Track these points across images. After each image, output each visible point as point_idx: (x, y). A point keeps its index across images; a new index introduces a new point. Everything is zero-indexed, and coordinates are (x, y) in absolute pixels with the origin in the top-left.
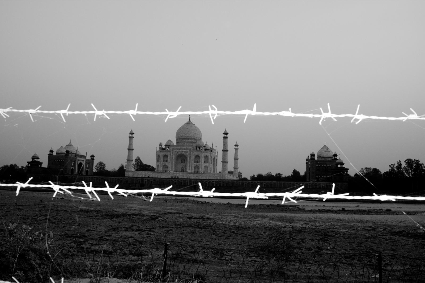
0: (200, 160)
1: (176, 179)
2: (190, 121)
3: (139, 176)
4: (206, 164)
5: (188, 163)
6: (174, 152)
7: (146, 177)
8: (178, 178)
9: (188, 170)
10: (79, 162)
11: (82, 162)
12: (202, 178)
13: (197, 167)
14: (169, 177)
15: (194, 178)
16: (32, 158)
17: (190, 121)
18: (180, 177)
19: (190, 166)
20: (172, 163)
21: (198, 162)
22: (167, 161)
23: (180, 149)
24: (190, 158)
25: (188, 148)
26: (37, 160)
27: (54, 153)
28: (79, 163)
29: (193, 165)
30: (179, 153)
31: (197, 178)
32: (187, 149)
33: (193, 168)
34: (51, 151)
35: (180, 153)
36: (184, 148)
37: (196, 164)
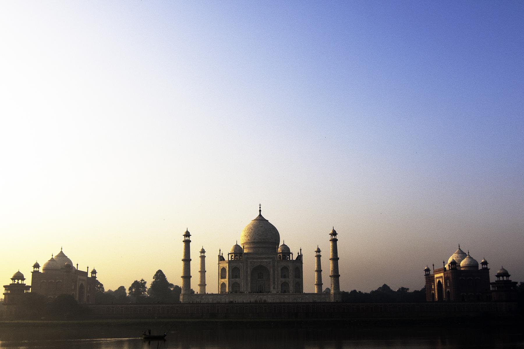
0: (290, 274)
2: (260, 215)
3: (203, 302)
5: (271, 278)
6: (249, 262)
7: (215, 302)
9: (272, 289)
10: (81, 282)
11: (84, 283)
12: (303, 301)
13: (285, 285)
14: (252, 300)
15: (291, 301)
16: (12, 279)
17: (260, 215)
18: (269, 301)
19: (274, 283)
20: (247, 280)
21: (284, 277)
22: (236, 277)
24: (274, 271)
26: (20, 282)
27: (41, 270)
28: (80, 284)
31: (295, 301)
32: (268, 258)
33: (280, 287)
34: (37, 266)
36: (264, 256)
37: (283, 280)
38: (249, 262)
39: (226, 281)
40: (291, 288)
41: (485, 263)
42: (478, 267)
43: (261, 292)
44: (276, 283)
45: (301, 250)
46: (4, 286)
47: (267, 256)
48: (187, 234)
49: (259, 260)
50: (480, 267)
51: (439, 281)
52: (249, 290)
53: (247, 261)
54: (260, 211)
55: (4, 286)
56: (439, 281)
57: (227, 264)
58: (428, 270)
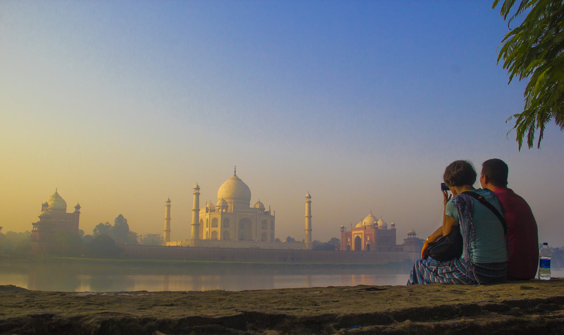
2: (235, 175)
17: (235, 175)
21: (263, 228)
39: (218, 229)
41: (394, 225)
42: (387, 227)
43: (242, 240)
46: (33, 224)
48: (198, 188)
50: (389, 228)
51: (358, 237)
54: (235, 171)
55: (33, 224)
56: (358, 237)
57: (220, 216)
58: (343, 228)
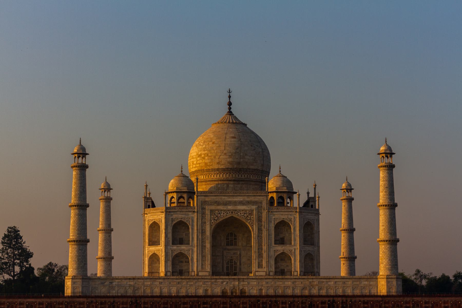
1: (236, 297)
2: (230, 113)
3: (113, 293)
4: (309, 248)
6: (208, 212)
8: (243, 295)
13: (283, 258)
17: (230, 113)
20: (203, 247)
22: (181, 242)
23: (226, 204)
24: (260, 230)
25: (252, 199)
29: (272, 253)
30: (224, 216)
32: (248, 203)
33: (273, 262)
35: (229, 215)
37: (280, 248)
38: (208, 212)
39: (160, 249)
40: (296, 265)
44: (265, 255)
45: (315, 185)
47: (247, 199)
49: (230, 207)
52: (208, 268)
53: (203, 209)
54: (230, 104)
57: (163, 215)
